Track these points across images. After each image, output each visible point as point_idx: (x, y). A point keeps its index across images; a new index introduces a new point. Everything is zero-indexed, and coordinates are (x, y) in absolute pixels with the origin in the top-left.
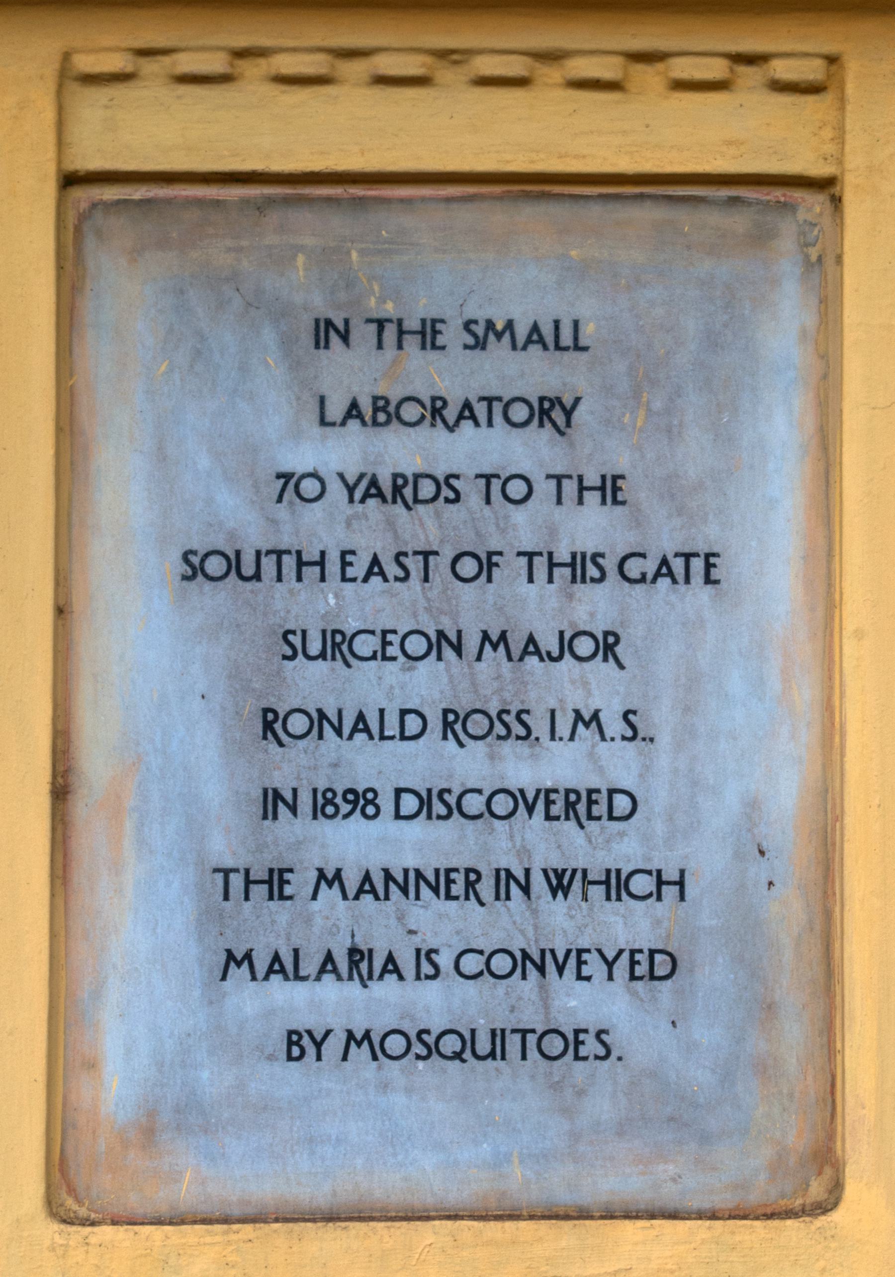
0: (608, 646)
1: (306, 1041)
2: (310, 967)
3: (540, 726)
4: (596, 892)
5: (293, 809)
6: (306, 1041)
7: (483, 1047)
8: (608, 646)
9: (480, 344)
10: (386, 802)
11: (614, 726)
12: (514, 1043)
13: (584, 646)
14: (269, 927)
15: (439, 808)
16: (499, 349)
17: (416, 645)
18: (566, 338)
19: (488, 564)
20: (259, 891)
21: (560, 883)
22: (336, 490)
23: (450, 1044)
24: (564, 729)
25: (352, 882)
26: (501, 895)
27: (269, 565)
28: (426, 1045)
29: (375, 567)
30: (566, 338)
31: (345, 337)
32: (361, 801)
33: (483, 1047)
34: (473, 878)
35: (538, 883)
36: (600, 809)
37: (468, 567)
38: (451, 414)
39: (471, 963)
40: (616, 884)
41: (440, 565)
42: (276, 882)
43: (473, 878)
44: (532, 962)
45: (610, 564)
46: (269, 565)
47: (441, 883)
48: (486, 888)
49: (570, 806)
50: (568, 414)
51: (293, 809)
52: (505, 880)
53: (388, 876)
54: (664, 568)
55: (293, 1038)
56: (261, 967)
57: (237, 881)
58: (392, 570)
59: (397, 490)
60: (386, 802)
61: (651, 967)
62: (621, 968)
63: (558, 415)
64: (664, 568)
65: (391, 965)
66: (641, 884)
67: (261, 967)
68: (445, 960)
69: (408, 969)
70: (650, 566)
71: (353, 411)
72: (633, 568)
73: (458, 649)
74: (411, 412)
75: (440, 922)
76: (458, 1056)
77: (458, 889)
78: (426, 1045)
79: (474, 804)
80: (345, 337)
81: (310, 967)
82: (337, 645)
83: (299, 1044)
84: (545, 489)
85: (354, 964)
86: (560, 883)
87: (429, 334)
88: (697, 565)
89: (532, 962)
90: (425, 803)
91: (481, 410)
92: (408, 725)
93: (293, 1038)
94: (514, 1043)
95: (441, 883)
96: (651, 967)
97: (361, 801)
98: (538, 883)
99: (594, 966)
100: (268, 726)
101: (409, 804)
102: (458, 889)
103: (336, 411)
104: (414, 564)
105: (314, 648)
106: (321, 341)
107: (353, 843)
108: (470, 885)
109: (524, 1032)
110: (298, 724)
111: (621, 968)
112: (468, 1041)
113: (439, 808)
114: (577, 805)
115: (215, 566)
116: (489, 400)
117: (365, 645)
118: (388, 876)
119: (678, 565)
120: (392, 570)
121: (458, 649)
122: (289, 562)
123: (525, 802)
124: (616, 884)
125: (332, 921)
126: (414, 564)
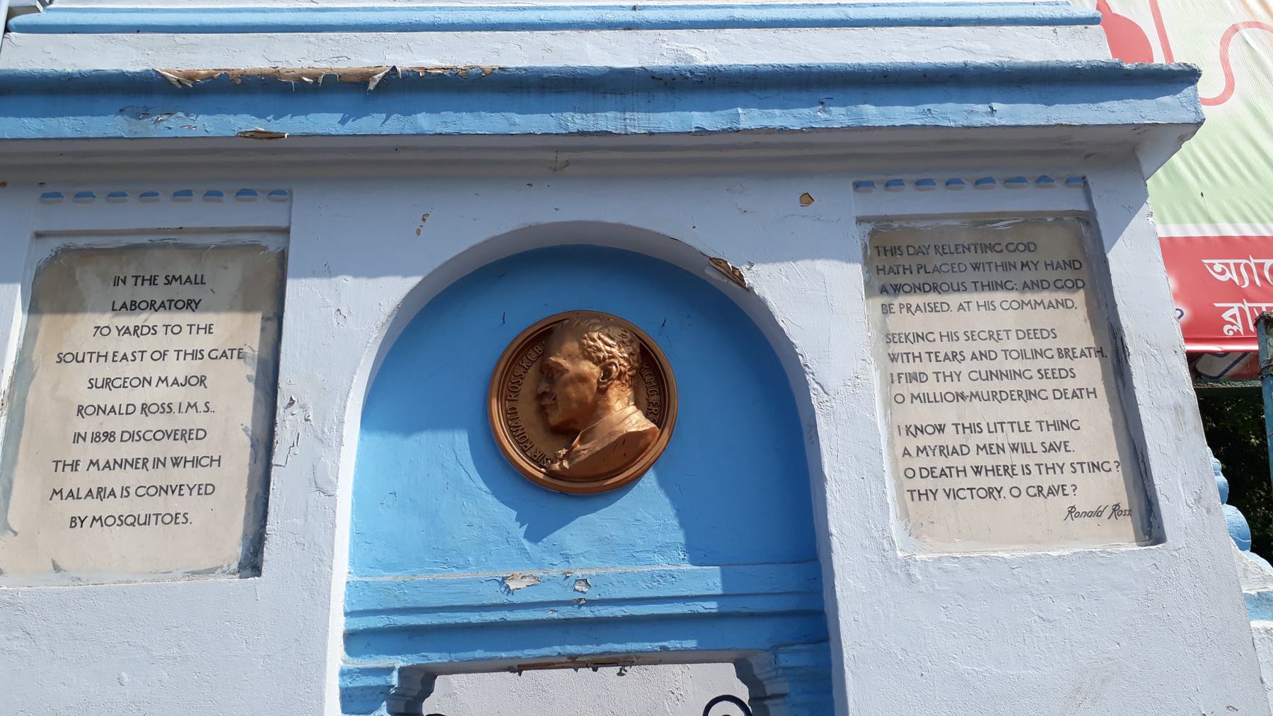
0: (202, 381)
1: (78, 521)
2: (82, 494)
3: (175, 408)
4: (189, 465)
5: (84, 439)
6: (78, 521)
7: (142, 521)
8: (202, 381)
9: (169, 283)
10: (118, 436)
11: (201, 407)
12: (153, 518)
13: (194, 381)
14: (70, 481)
15: (136, 437)
17: (135, 382)
18: (199, 280)
19: (163, 355)
20: (68, 469)
21: (176, 462)
22: (114, 332)
23: (130, 520)
24: (183, 409)
25: (102, 464)
26: (155, 466)
27: (87, 357)
28: (122, 521)
29: (125, 357)
30: (199, 280)
31: (124, 282)
32: (109, 436)
33: (142, 521)
34: (145, 461)
35: (169, 463)
36: (193, 436)
37: (156, 356)
38: (157, 306)
39: (141, 491)
40: (196, 462)
41: (147, 356)
42: (75, 465)
43: (145, 461)
44: (163, 490)
45: (205, 354)
46: (87, 357)
47: (133, 464)
48: (150, 465)
49: (183, 435)
50: (196, 305)
51: (84, 439)
52: (157, 462)
53: (115, 462)
54: (224, 354)
55: (73, 520)
56: (65, 495)
57: (60, 465)
58: (130, 357)
59: (135, 331)
60: (118, 436)
61: (205, 490)
62: (195, 491)
63: (193, 305)
64: (224, 354)
65: (113, 493)
66: (205, 462)
67: (65, 495)
68: (132, 491)
69: (118, 493)
70: (219, 353)
71: (124, 306)
72: (213, 355)
73: (150, 383)
74: (143, 305)
75: (131, 477)
76: (132, 524)
77: (140, 465)
78: (122, 521)
80: (124, 282)
81: (82, 494)
82: (108, 383)
84: (186, 329)
85: (99, 493)
86: (176, 462)
87: (153, 281)
88: (235, 353)
89: (163, 490)
90: (132, 436)
91: (167, 304)
92: (129, 410)
93: (73, 520)
94: (153, 518)
95: (133, 464)
96: (205, 490)
97: (109, 436)
98: (169, 463)
99: (185, 491)
100: (79, 411)
101: (126, 436)
102: (140, 465)
103: (117, 306)
104: (138, 355)
105: (99, 384)
106: (116, 284)
107: (105, 451)
108: (144, 464)
109: (157, 515)
111: (195, 491)
112: (137, 519)
113: (136, 437)
114: (186, 435)
115: (69, 358)
116: (171, 301)
117: (117, 383)
118: (115, 462)
119: (229, 353)
120: (130, 357)
121: (150, 383)
122: (95, 356)
124: (196, 462)
126: (138, 355)
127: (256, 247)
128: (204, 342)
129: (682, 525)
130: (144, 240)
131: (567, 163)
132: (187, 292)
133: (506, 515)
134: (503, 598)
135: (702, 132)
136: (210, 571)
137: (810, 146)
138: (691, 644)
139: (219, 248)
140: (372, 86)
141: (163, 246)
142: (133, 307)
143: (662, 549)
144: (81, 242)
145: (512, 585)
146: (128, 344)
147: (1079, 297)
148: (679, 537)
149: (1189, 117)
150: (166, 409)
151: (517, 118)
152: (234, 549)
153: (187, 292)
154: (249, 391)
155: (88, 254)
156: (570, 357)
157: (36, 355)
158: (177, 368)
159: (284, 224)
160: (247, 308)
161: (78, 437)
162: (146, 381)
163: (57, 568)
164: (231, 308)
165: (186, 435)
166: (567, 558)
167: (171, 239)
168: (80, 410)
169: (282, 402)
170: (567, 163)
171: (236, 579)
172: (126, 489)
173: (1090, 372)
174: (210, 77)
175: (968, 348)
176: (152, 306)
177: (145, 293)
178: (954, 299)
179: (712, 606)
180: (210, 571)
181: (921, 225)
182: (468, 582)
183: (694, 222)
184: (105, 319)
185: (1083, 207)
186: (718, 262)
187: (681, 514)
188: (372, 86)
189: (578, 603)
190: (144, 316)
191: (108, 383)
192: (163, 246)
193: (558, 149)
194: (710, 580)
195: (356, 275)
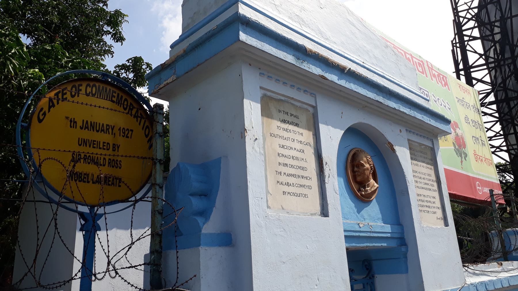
0: (303, 152)
16: (292, 117)
29: (285, 139)
42: (280, 173)
61: (310, 187)
65: (290, 185)
66: (308, 178)
79: (295, 167)
82: (283, 147)
83: (284, 193)
87: (287, 113)
89: (301, 186)
96: (310, 187)
97: (286, 165)
110: (281, 155)
114: (303, 169)
123: (300, 167)
124: (306, 178)
125: (284, 179)
127: (307, 110)
128: (300, 138)
129: (381, 213)
130: (283, 98)
131: (366, 106)
132: (295, 120)
133: (353, 205)
134: (359, 229)
135: (395, 109)
136: (315, 214)
137: (403, 117)
138: (385, 245)
139: (300, 107)
140: (346, 72)
141: (288, 102)
142: (284, 121)
143: (378, 219)
144: (269, 94)
145: (361, 226)
146: (286, 134)
147: (432, 167)
148: (380, 216)
149: (450, 132)
150: (297, 159)
151: (368, 92)
152: (318, 208)
153: (295, 120)
154: (313, 156)
155: (271, 98)
156: (365, 162)
157: (265, 132)
158: (298, 146)
159: (314, 105)
160: (309, 130)
161: (280, 164)
162: (291, 148)
163: (283, 209)
164: (306, 129)
165: (303, 169)
166: (364, 219)
167: (290, 100)
168: (279, 154)
169: (324, 164)
170: (366, 106)
171: (320, 217)
172: (293, 184)
173: (435, 184)
174: (315, 53)
175: (423, 176)
176: (288, 122)
177: (287, 118)
178: (419, 163)
179: (389, 235)
180: (315, 214)
181: (413, 143)
182: (352, 224)
183: (390, 132)
184: (279, 123)
185: (431, 146)
186: (389, 143)
187: (380, 210)
188: (346, 72)
189: (370, 232)
190: (288, 125)
191: (283, 147)
192: (288, 102)
193: (368, 103)
194: (388, 228)
195: (332, 127)
